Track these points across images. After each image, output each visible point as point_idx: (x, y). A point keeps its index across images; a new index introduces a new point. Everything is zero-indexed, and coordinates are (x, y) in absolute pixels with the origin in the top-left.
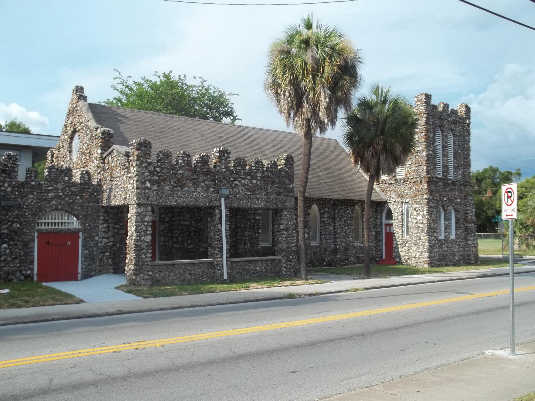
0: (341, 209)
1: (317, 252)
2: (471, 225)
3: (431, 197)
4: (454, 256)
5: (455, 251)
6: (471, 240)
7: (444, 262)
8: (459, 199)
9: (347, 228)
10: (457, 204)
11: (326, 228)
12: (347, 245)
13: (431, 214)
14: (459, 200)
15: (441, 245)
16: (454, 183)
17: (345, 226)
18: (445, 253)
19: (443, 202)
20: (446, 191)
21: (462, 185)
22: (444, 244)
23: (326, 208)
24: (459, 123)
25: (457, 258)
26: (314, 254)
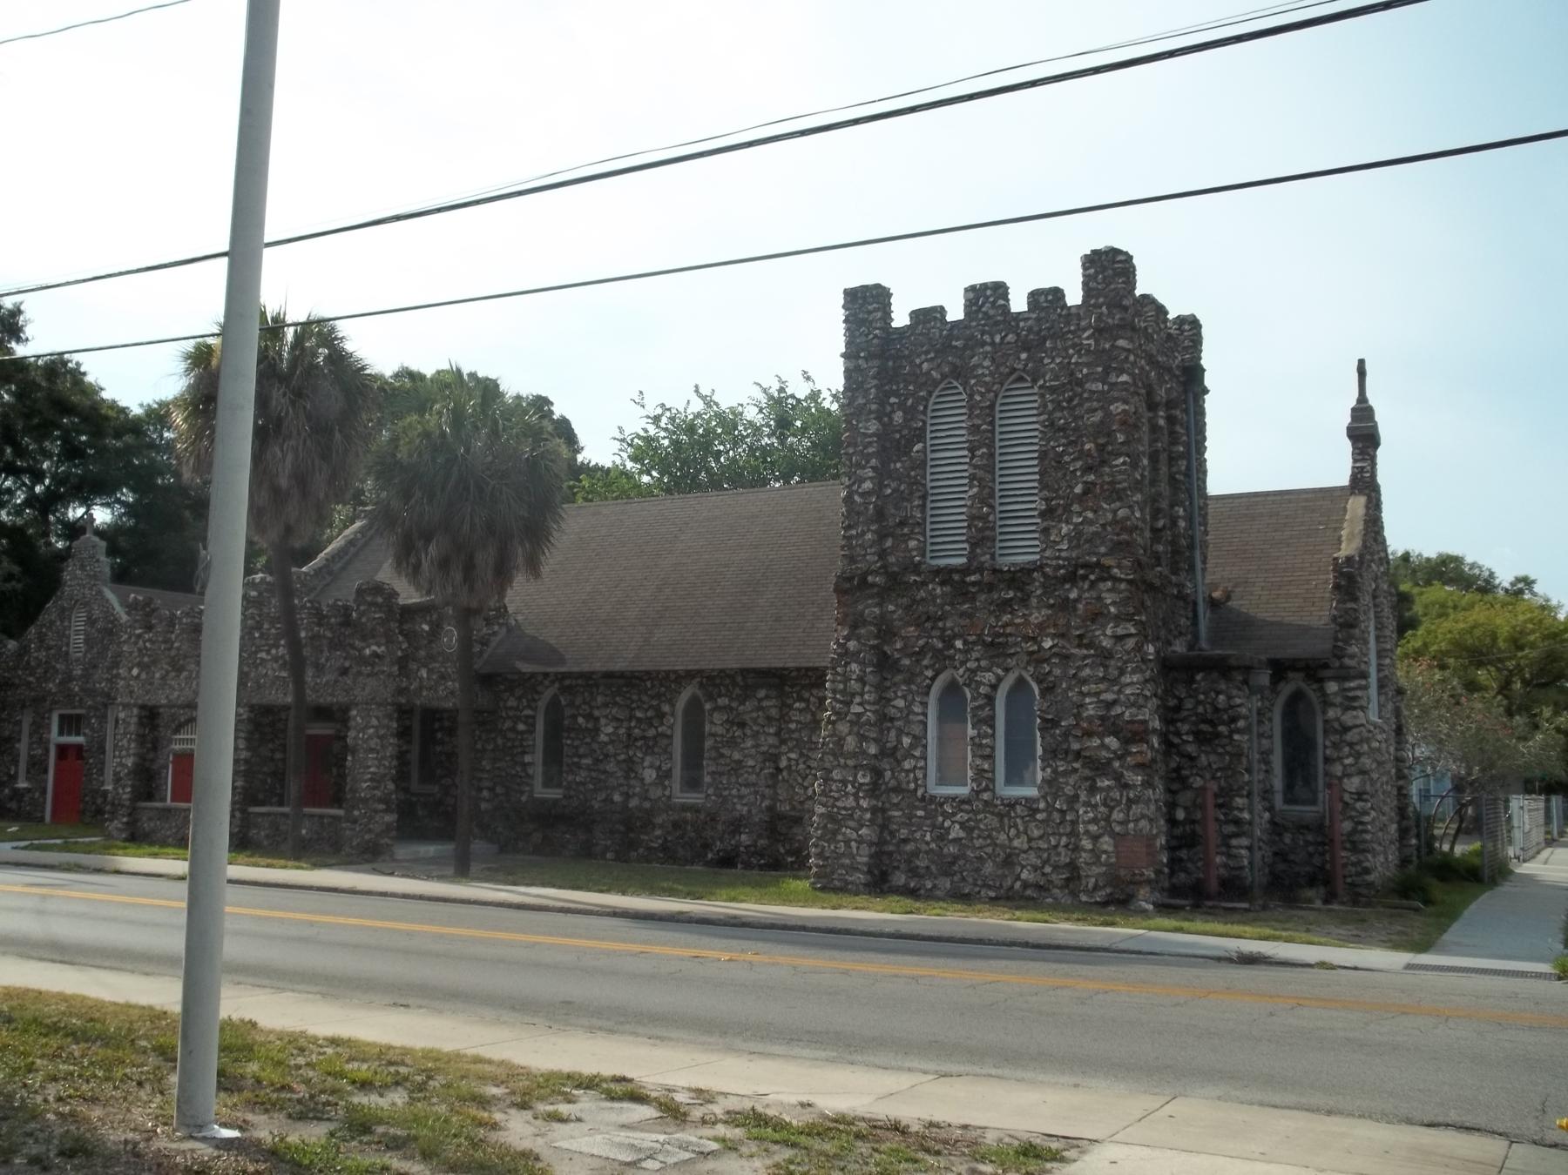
0: (767, 697)
1: (686, 822)
2: (1096, 742)
3: (852, 645)
4: (1009, 861)
5: (1016, 843)
6: (1087, 804)
7: (946, 883)
8: (1054, 636)
9: (793, 756)
10: (1037, 658)
11: (722, 756)
12: (793, 808)
13: (848, 704)
14: (1048, 644)
15: (930, 816)
16: (1018, 578)
17: (791, 750)
18: (952, 849)
19: (952, 658)
20: (963, 615)
21: (1064, 580)
22: (946, 816)
23: (720, 696)
24: (1054, 337)
25: (1024, 875)
26: (676, 825)
